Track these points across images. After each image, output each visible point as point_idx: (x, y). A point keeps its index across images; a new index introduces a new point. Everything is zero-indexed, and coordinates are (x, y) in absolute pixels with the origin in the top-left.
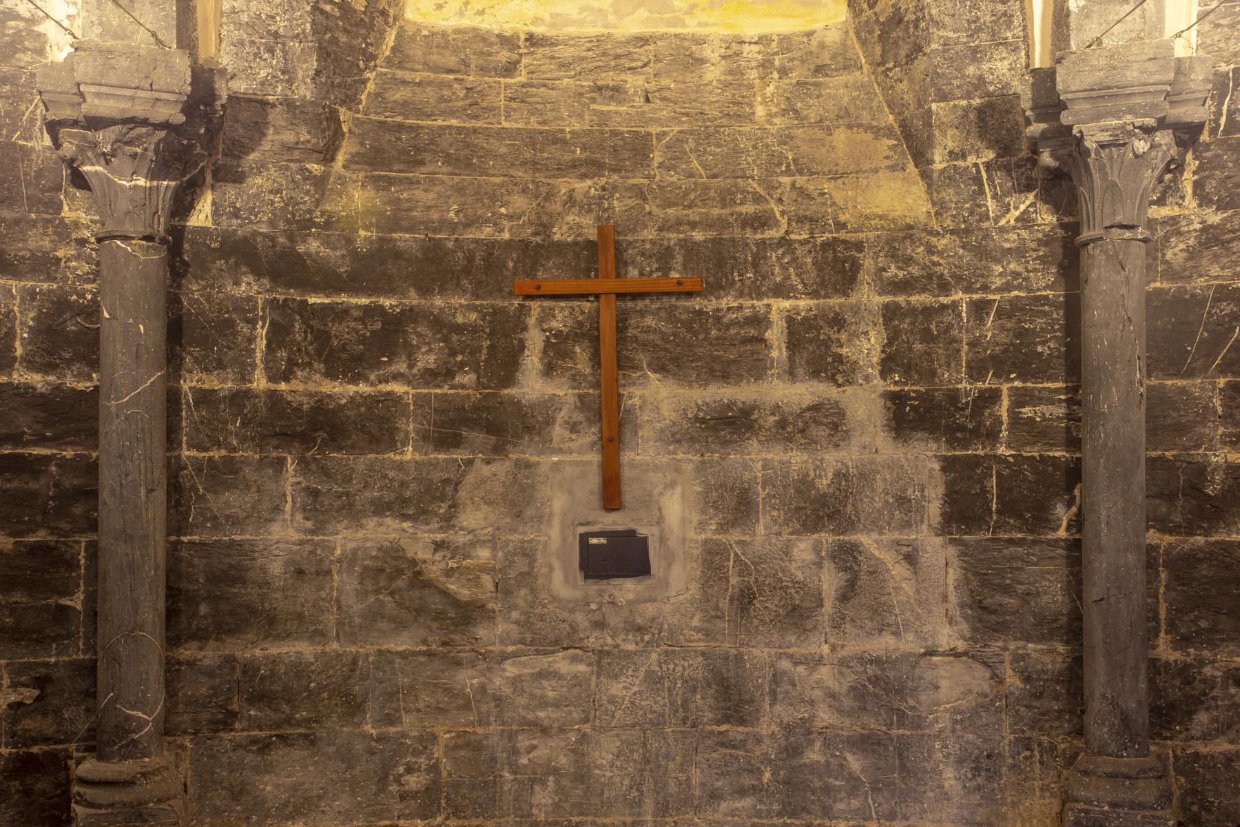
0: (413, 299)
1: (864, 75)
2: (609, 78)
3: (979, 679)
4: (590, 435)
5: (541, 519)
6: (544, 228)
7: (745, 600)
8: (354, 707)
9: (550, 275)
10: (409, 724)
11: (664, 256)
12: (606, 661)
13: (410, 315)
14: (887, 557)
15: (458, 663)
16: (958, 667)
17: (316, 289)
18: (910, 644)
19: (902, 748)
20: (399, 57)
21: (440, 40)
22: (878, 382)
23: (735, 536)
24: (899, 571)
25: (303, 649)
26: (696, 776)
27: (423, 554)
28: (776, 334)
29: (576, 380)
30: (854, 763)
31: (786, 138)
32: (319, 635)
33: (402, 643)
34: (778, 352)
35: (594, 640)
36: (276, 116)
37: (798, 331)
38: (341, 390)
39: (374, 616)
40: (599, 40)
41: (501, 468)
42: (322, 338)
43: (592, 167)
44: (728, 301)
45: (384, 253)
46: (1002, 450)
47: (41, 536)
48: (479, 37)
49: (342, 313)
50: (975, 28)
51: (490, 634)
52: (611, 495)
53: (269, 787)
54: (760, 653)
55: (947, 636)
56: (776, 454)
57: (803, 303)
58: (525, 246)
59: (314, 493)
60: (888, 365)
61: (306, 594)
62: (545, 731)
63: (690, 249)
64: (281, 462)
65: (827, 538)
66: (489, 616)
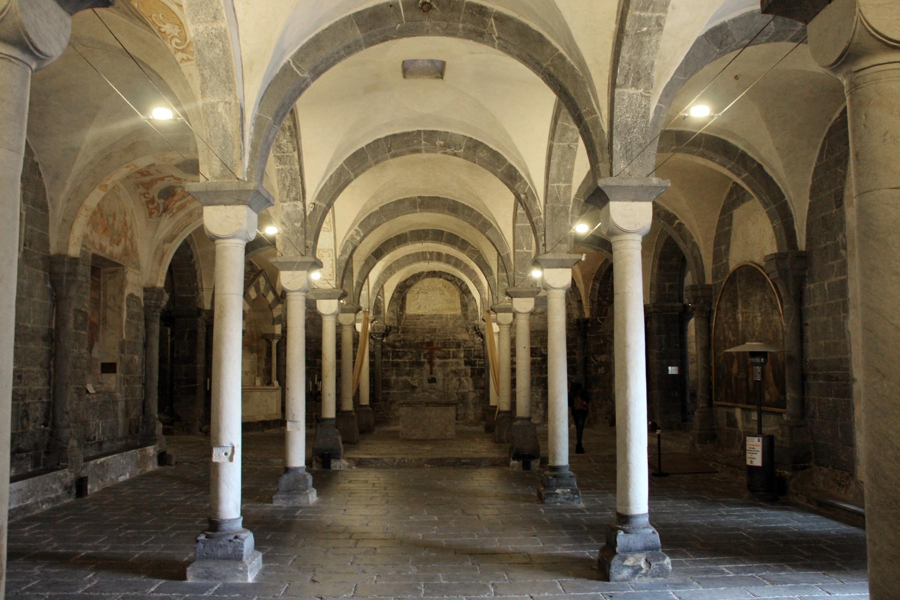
1: (462, 320)
2: (431, 320)
3: (475, 394)
9: (424, 346)
18: (467, 391)
20: (406, 318)
21: (410, 316)
29: (428, 359)
31: (453, 328)
34: (451, 356)
35: (430, 390)
40: (430, 315)
42: (398, 355)
43: (429, 332)
46: (477, 367)
49: (400, 351)
50: (473, 317)
52: (431, 373)
53: (392, 408)
55: (471, 389)
57: (455, 350)
60: (464, 357)
63: (441, 343)
64: (393, 370)
65: (457, 378)
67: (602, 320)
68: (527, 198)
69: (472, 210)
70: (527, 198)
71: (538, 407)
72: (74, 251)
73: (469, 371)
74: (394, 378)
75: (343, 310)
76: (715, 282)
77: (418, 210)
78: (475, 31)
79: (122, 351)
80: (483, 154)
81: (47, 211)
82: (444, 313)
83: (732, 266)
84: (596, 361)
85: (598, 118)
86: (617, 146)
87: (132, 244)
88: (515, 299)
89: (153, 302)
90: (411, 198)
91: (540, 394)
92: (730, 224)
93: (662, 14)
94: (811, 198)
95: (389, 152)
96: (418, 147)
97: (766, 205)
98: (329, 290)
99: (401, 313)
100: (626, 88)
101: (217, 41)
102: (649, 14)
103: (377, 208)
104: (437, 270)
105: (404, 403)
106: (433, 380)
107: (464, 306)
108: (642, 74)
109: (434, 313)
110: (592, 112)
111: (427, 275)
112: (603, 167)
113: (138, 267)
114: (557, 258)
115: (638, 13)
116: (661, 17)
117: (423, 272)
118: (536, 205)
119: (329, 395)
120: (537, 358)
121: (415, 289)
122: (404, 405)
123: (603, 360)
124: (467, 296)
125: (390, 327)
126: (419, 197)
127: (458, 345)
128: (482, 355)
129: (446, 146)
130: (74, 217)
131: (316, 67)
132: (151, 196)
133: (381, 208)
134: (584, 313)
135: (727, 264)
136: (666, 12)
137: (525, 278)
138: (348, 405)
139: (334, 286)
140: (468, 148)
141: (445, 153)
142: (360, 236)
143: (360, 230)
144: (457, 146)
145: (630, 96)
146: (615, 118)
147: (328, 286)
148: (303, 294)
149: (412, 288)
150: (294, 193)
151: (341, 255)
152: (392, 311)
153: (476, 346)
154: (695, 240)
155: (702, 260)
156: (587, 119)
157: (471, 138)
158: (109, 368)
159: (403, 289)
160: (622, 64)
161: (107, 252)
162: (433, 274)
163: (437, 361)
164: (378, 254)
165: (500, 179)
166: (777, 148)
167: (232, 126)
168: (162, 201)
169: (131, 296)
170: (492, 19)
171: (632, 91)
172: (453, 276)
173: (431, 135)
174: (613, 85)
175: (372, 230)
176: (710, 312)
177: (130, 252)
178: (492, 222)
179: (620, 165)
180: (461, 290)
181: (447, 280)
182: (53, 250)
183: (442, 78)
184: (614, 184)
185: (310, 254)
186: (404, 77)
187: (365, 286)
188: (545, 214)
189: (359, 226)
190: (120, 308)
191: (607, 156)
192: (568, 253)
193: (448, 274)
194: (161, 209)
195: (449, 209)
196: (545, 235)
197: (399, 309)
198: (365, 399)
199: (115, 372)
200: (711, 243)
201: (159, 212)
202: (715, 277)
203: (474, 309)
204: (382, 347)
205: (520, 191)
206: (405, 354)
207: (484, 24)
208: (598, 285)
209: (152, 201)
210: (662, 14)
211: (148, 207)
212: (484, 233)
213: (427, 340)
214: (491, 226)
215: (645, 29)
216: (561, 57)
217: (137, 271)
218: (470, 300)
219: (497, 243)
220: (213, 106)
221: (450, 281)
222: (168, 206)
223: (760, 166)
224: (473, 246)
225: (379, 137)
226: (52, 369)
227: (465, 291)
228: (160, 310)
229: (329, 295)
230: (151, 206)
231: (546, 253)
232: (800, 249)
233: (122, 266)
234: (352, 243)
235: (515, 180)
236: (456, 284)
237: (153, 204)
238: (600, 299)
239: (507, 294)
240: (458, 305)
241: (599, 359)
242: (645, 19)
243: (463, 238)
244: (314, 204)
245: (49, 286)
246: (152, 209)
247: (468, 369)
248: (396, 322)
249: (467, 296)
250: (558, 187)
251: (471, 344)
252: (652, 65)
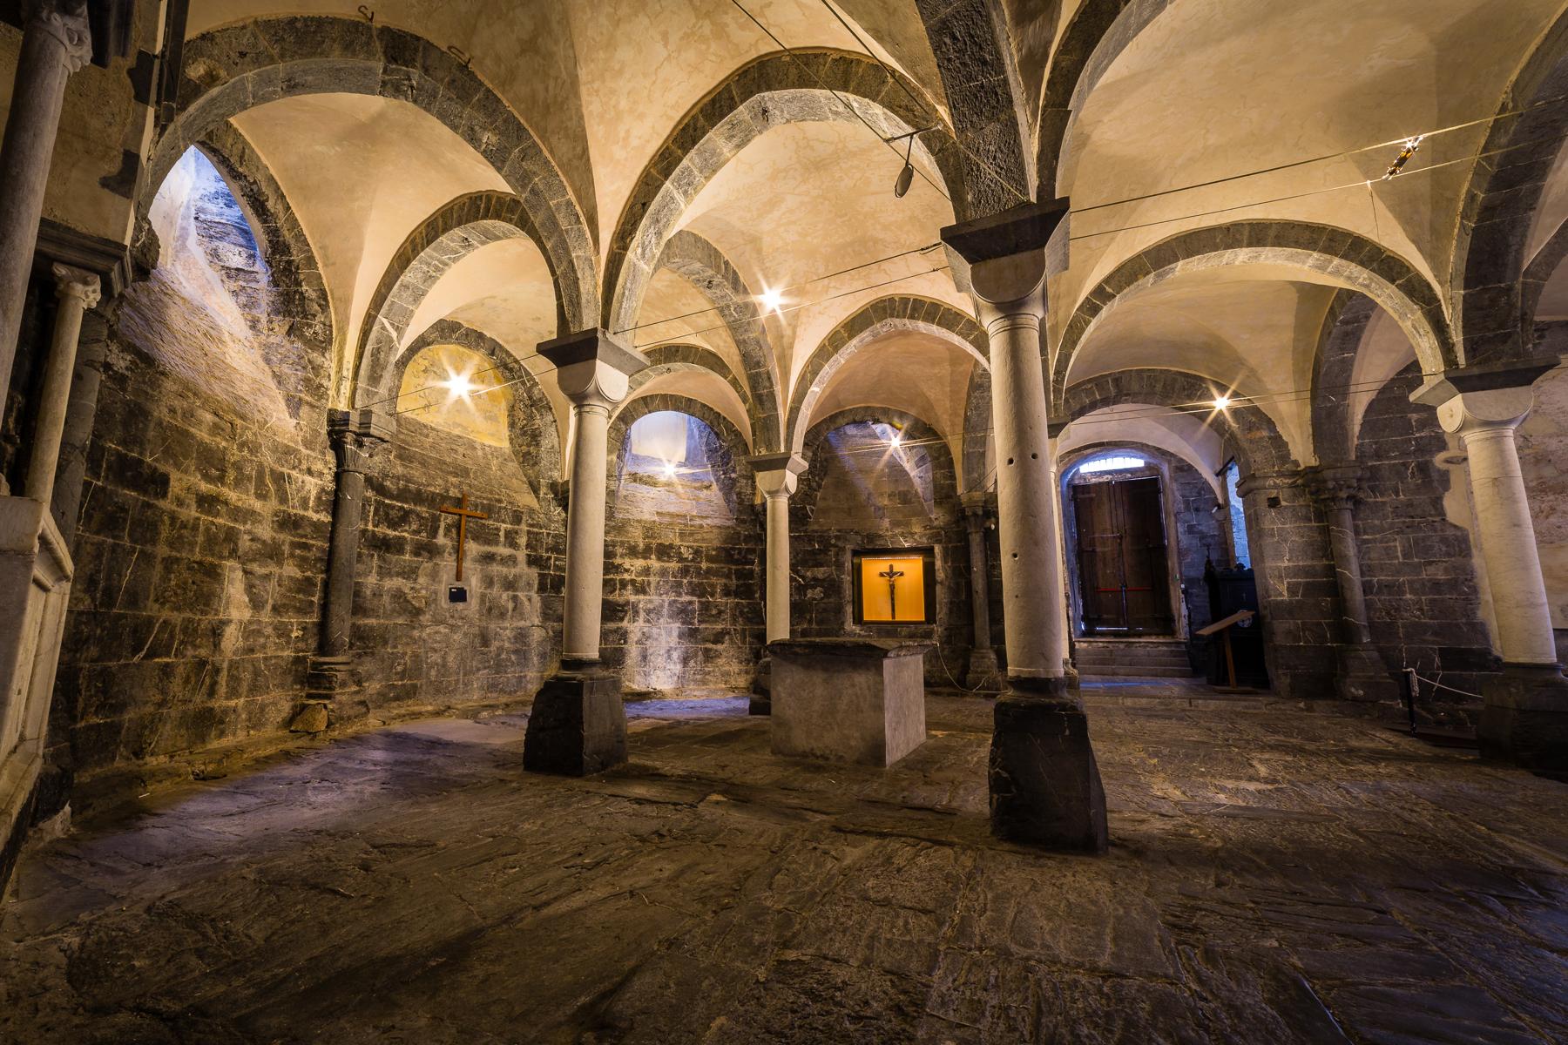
0: (412, 507)
2: (454, 447)
4: (454, 557)
5: (440, 582)
6: (447, 491)
7: (490, 610)
8: (385, 643)
10: (400, 649)
11: (476, 506)
12: (453, 628)
13: (411, 511)
14: (524, 599)
15: (414, 628)
16: (538, 630)
18: (528, 624)
19: (525, 652)
22: (526, 552)
23: (488, 591)
24: (527, 603)
25: (372, 621)
26: (474, 663)
27: (407, 591)
28: (502, 534)
29: (452, 539)
30: (513, 657)
32: (378, 617)
33: (400, 621)
34: (502, 539)
35: (451, 621)
37: (508, 533)
38: (392, 533)
39: (394, 610)
41: (430, 565)
42: (387, 514)
44: (491, 522)
45: (406, 490)
47: (309, 574)
48: (419, 423)
49: (393, 507)
51: (425, 618)
52: (458, 577)
54: (492, 626)
55: (537, 621)
56: (500, 568)
58: (441, 495)
59: (380, 567)
60: (528, 546)
61: (376, 602)
62: (436, 651)
63: (483, 505)
65: (510, 593)
66: (424, 612)
71: (669, 657)
74: (372, 580)
84: (803, 578)
91: (675, 633)
106: (458, 596)
109: (457, 432)
120: (671, 565)
123: (820, 576)
127: (517, 518)
163: (473, 548)
206: (405, 517)
213: (453, 492)
218: (546, 425)
241: (809, 574)
247: (534, 572)
251: (542, 519)
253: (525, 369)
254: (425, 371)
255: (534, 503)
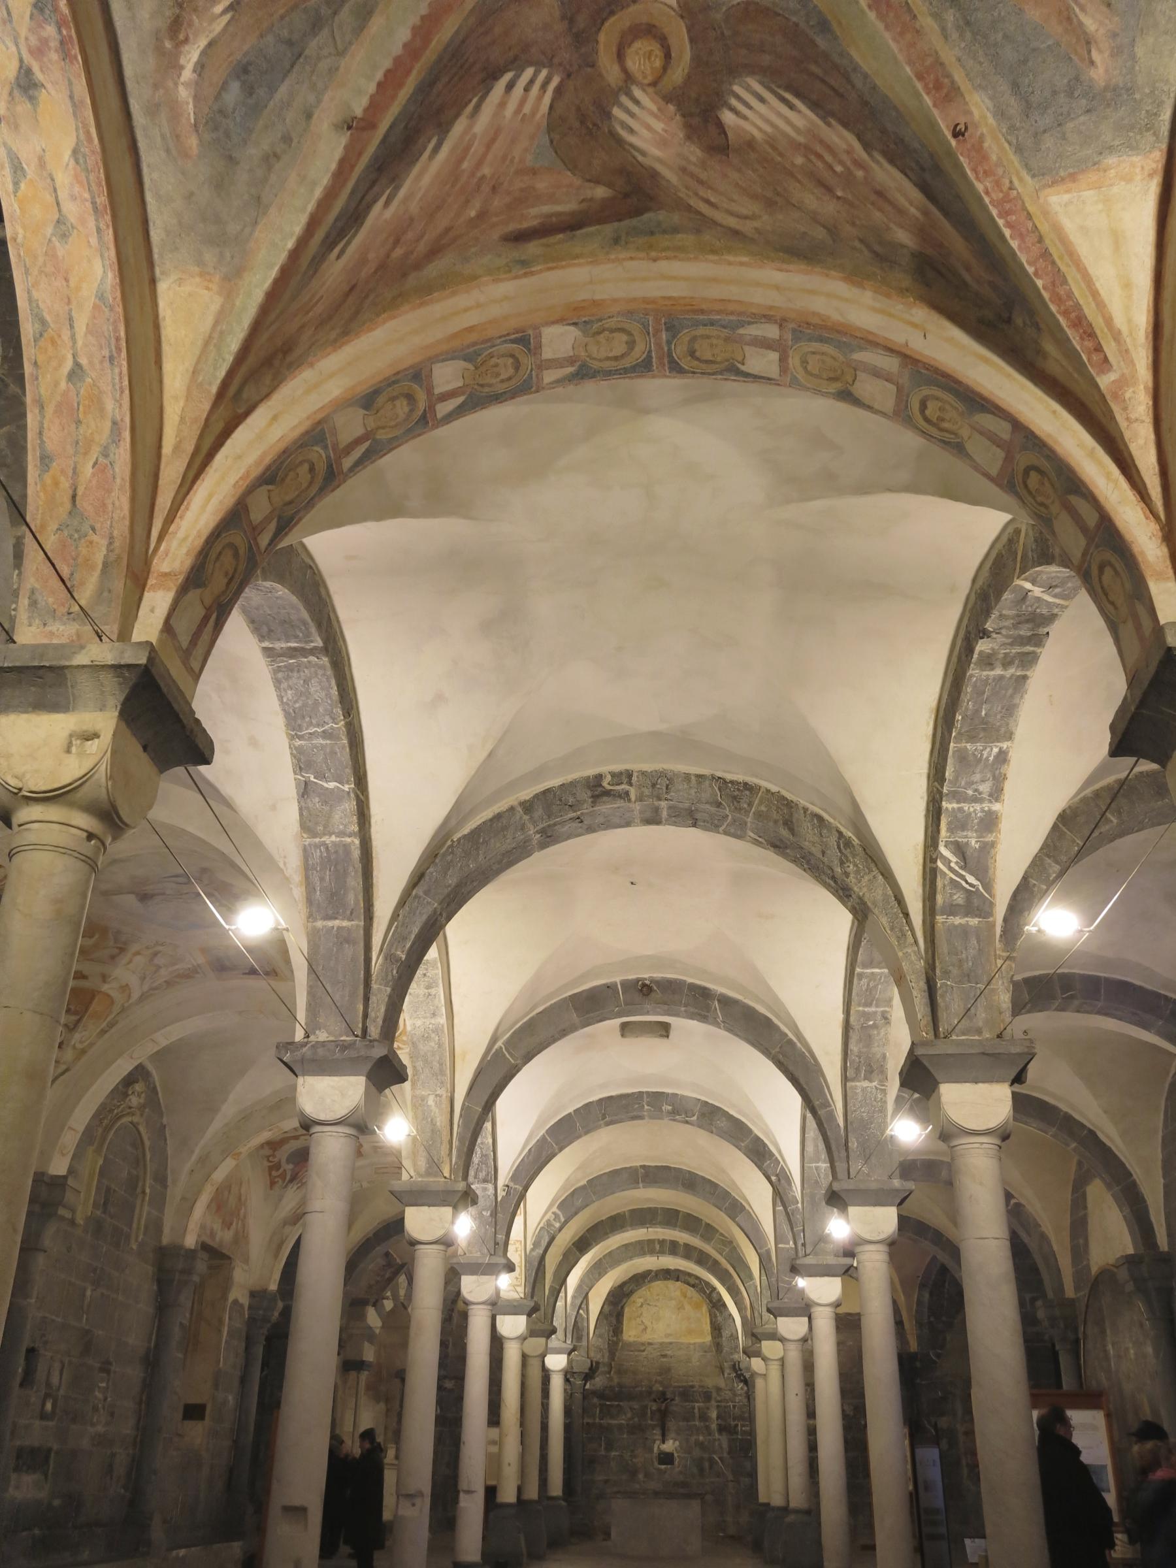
6: (651, 1388)
17: (608, 1400)
36: (601, 1365)
49: (611, 1406)
60: (718, 1418)
67: (938, 1356)
68: (779, 1180)
69: (715, 1186)
70: (779, 1180)
72: (190, 1241)
73: (725, 1445)
75: (532, 1333)
76: (1078, 1295)
77: (641, 1185)
78: (700, 1015)
79: (216, 1386)
80: (723, 1123)
81: (165, 1186)
82: (684, 1340)
83: (1094, 1270)
85: (833, 1110)
86: (853, 1144)
87: (244, 1226)
88: (779, 1319)
89: (261, 1312)
90: (631, 1167)
92: (1085, 1208)
93: (887, 1009)
94: (1164, 1177)
95: (603, 1119)
96: (640, 1114)
97: (1109, 1187)
98: (515, 1300)
99: (615, 1339)
100: (859, 1081)
101: (433, 1035)
102: (873, 1009)
103: (584, 1182)
104: (672, 1268)
105: (618, 1492)
107: (716, 1329)
108: (875, 1067)
110: (826, 1104)
111: (656, 1275)
112: (841, 1166)
113: (246, 1261)
114: (820, 1263)
115: (861, 1009)
116: (886, 1012)
117: (649, 1272)
118: (792, 1190)
119: (509, 1464)
121: (638, 1298)
122: (618, 1496)
124: (721, 1313)
125: (598, 1363)
126: (641, 1166)
127: (707, 1397)
128: (747, 1415)
129: (675, 1112)
130: (199, 1193)
131: (529, 1053)
132: (276, 1160)
133: (590, 1182)
134: (908, 1343)
135: (1088, 1267)
136: (891, 1006)
137: (792, 1289)
138: (532, 1493)
139: (522, 1296)
140: (702, 1115)
141: (674, 1120)
142: (560, 1222)
143: (559, 1213)
144: (688, 1113)
145: (864, 1089)
146: (849, 1114)
147: (515, 1296)
148: (489, 1307)
149: (634, 1297)
150: (484, 1173)
151: (532, 1250)
152: (600, 1336)
153: (737, 1399)
154: (1044, 1229)
155: (1056, 1259)
156: (821, 1112)
157: (707, 1102)
158: (194, 1412)
159: (618, 1299)
160: (852, 1057)
161: (217, 1239)
162: (668, 1274)
164: (582, 1245)
165: (745, 1154)
166: (1105, 1112)
167: (441, 1120)
168: (291, 1166)
169: (236, 1302)
170: (716, 1003)
171: (866, 1084)
172: (697, 1278)
173: (657, 1098)
174: (845, 1079)
175: (576, 1213)
176: (1077, 1341)
177: (241, 1238)
178: (744, 1203)
179: (857, 1165)
180: (711, 1301)
181: (688, 1284)
182: (165, 1240)
183: (668, 1037)
184: (851, 1187)
185: (501, 1253)
186: (622, 1035)
187: (562, 1294)
188: (803, 1203)
189: (559, 1207)
190: (221, 1321)
191: (843, 1154)
192: (836, 1255)
193: (690, 1275)
194: (288, 1178)
195: (684, 1185)
196: (804, 1231)
197: (611, 1333)
198: (556, 1486)
199: (202, 1418)
200: (1066, 1234)
201: (284, 1181)
202: (1077, 1288)
203: (732, 1335)
204: (584, 1398)
205: (770, 1172)
207: (708, 1008)
208: (927, 1296)
209: (277, 1166)
210: (887, 1009)
211: (270, 1175)
212: (733, 1219)
214: (743, 1208)
215: (871, 1023)
216: (790, 1042)
217: (246, 1267)
219: (754, 1234)
220: (423, 1099)
221: (693, 1286)
222: (297, 1174)
223: (1092, 1133)
224: (722, 1235)
225: (591, 1100)
226: (143, 1406)
227: (717, 1305)
228: (269, 1325)
229: (513, 1309)
230: (274, 1173)
231: (806, 1255)
232: (1161, 1249)
233: (229, 1258)
234: (548, 1232)
235: (764, 1156)
236: (701, 1291)
237: (278, 1170)
238: (932, 1319)
239: (769, 1311)
240: (707, 1327)
242: (869, 1013)
243: (708, 1221)
244: (508, 1186)
245: (155, 1287)
246: (276, 1177)
248: (607, 1355)
249: (721, 1313)
250: (817, 1168)
251: (728, 1394)
252: (884, 1056)
253: (704, 1281)
254: (641, 1306)
255: (722, 1383)
